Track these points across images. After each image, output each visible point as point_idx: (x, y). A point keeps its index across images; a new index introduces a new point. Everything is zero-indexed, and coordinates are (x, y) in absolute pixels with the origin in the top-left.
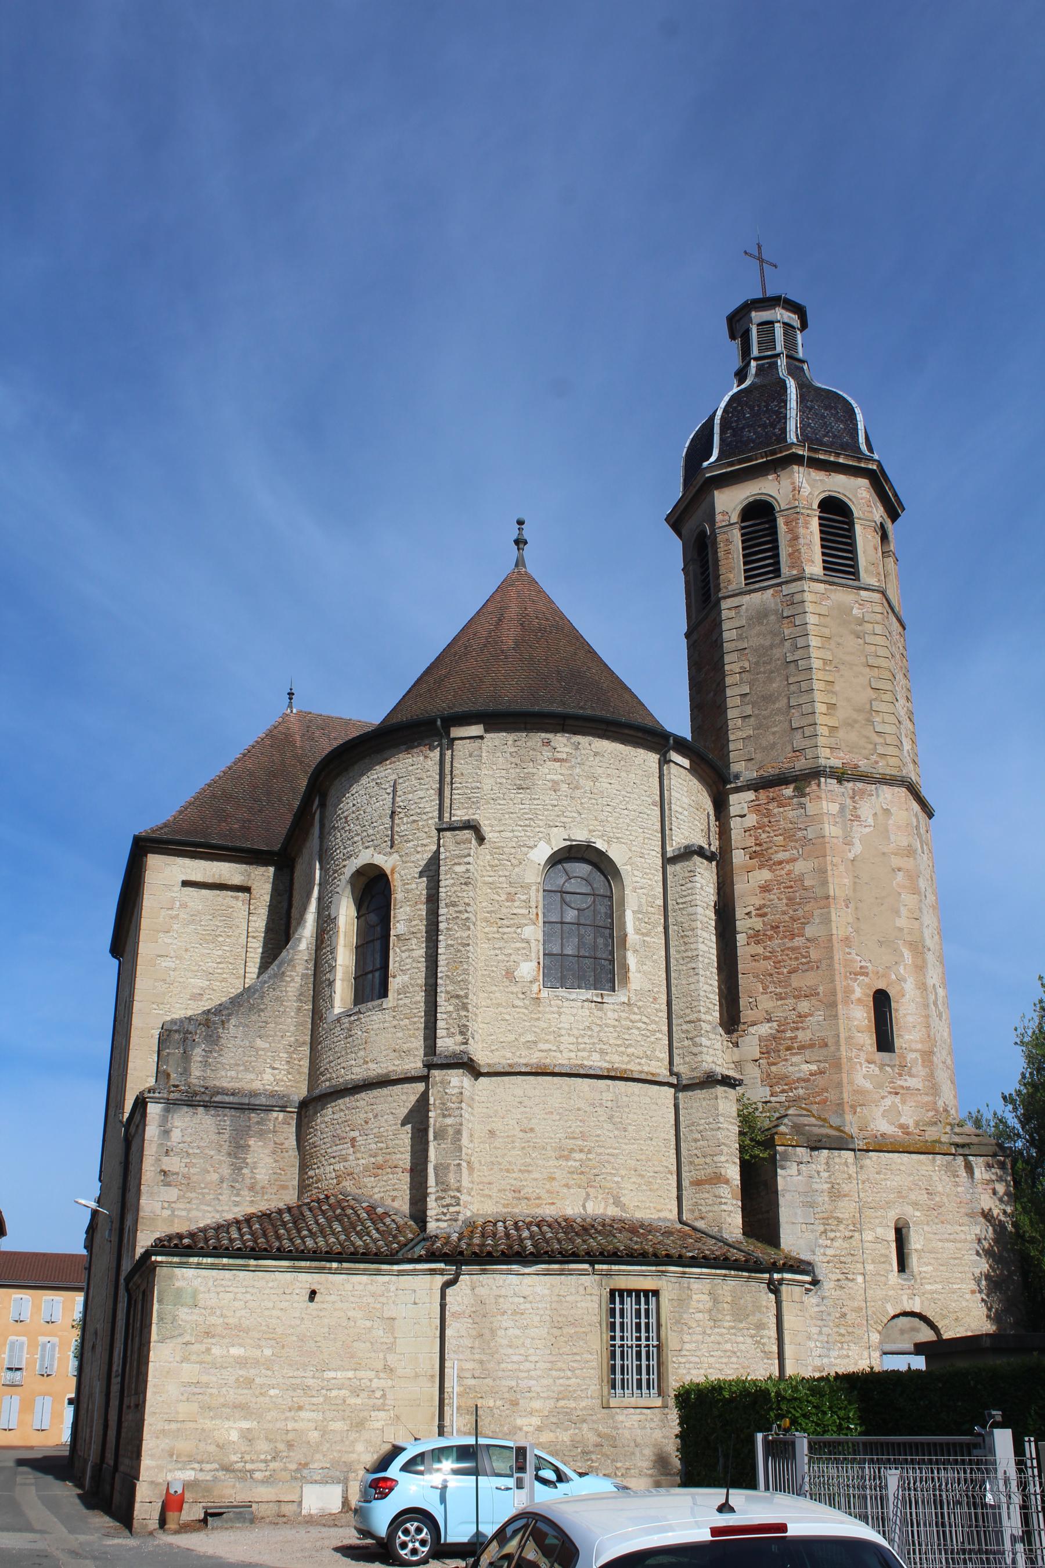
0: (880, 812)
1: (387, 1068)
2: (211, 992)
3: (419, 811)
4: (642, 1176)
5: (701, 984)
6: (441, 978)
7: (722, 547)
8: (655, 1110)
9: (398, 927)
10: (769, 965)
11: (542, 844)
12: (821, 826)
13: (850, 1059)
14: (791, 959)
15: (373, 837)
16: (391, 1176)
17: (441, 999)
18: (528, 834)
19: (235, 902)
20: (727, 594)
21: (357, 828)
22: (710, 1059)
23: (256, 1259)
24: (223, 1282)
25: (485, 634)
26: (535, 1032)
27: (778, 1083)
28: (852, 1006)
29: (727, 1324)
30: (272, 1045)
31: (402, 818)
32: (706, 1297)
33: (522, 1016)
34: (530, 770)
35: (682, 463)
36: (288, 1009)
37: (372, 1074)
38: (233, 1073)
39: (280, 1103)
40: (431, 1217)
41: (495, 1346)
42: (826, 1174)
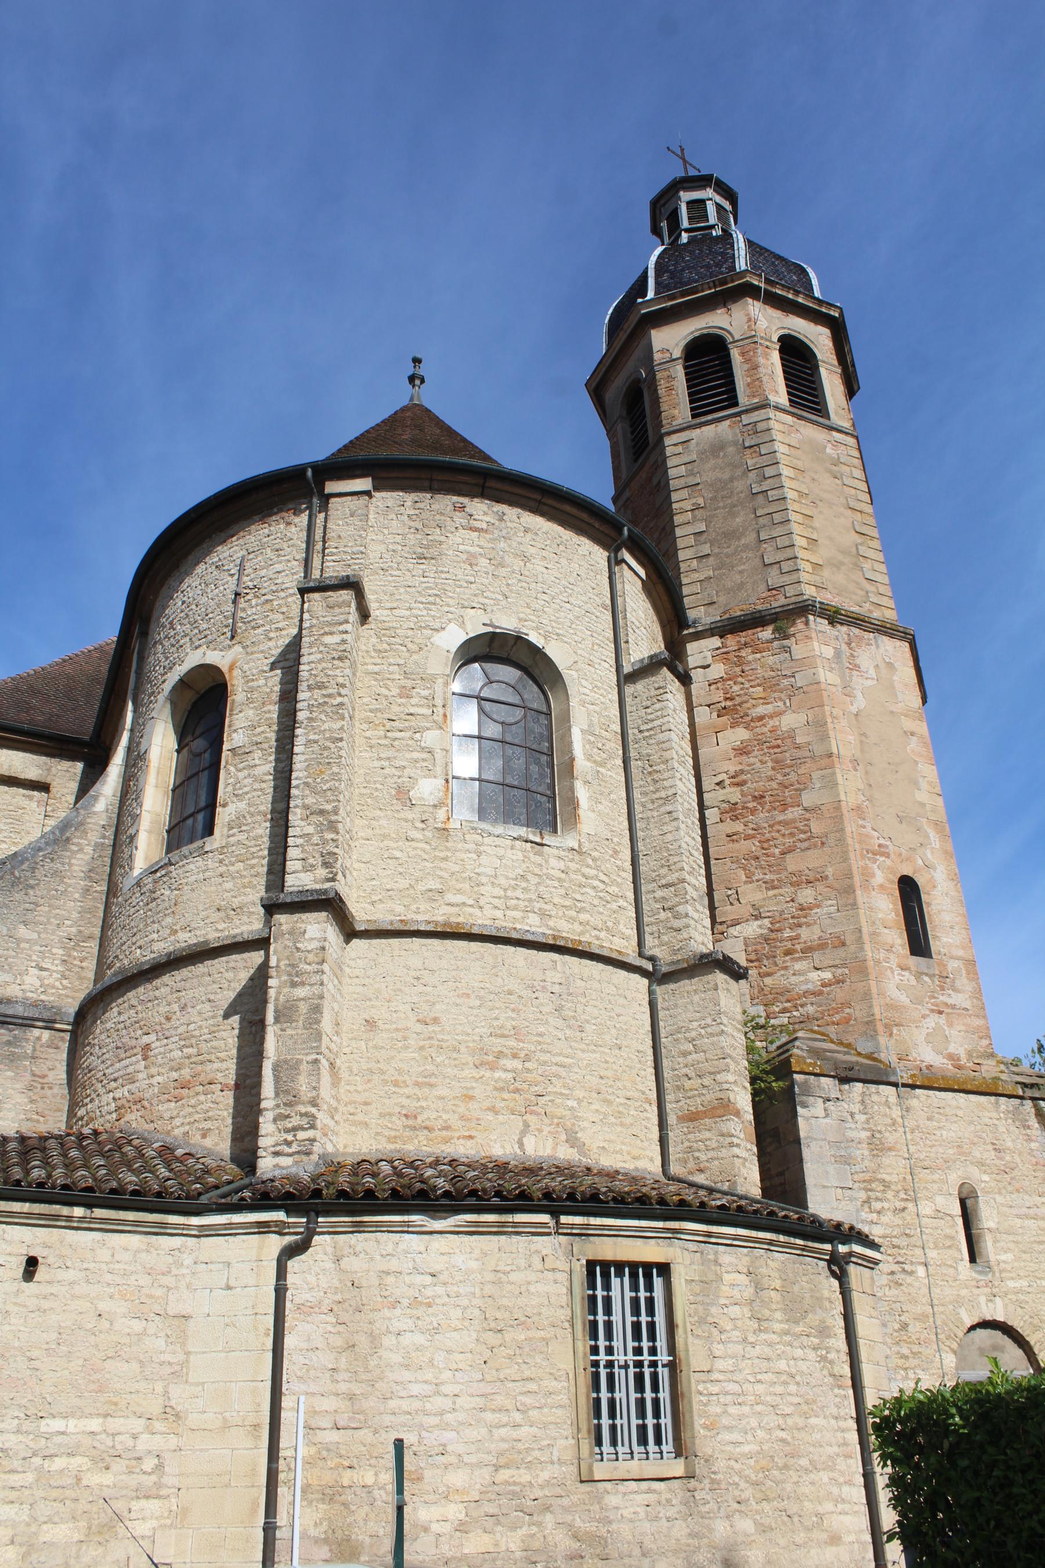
0: (882, 665)
1: (204, 936)
3: (274, 588)
4: (609, 1102)
5: (682, 833)
6: (297, 787)
8: (623, 1006)
9: (235, 737)
10: (752, 846)
11: (452, 627)
12: (813, 670)
13: (878, 962)
14: (784, 835)
16: (202, 1098)
17: (295, 817)
18: (433, 613)
19: (28, 802)
21: (184, 628)
22: (700, 939)
28: (874, 893)
29: (777, 1327)
30: (43, 936)
31: (249, 600)
32: (743, 1279)
33: (420, 852)
34: (437, 537)
36: (70, 889)
39: (46, 1015)
40: (265, 1149)
41: (378, 1366)
42: (862, 1118)
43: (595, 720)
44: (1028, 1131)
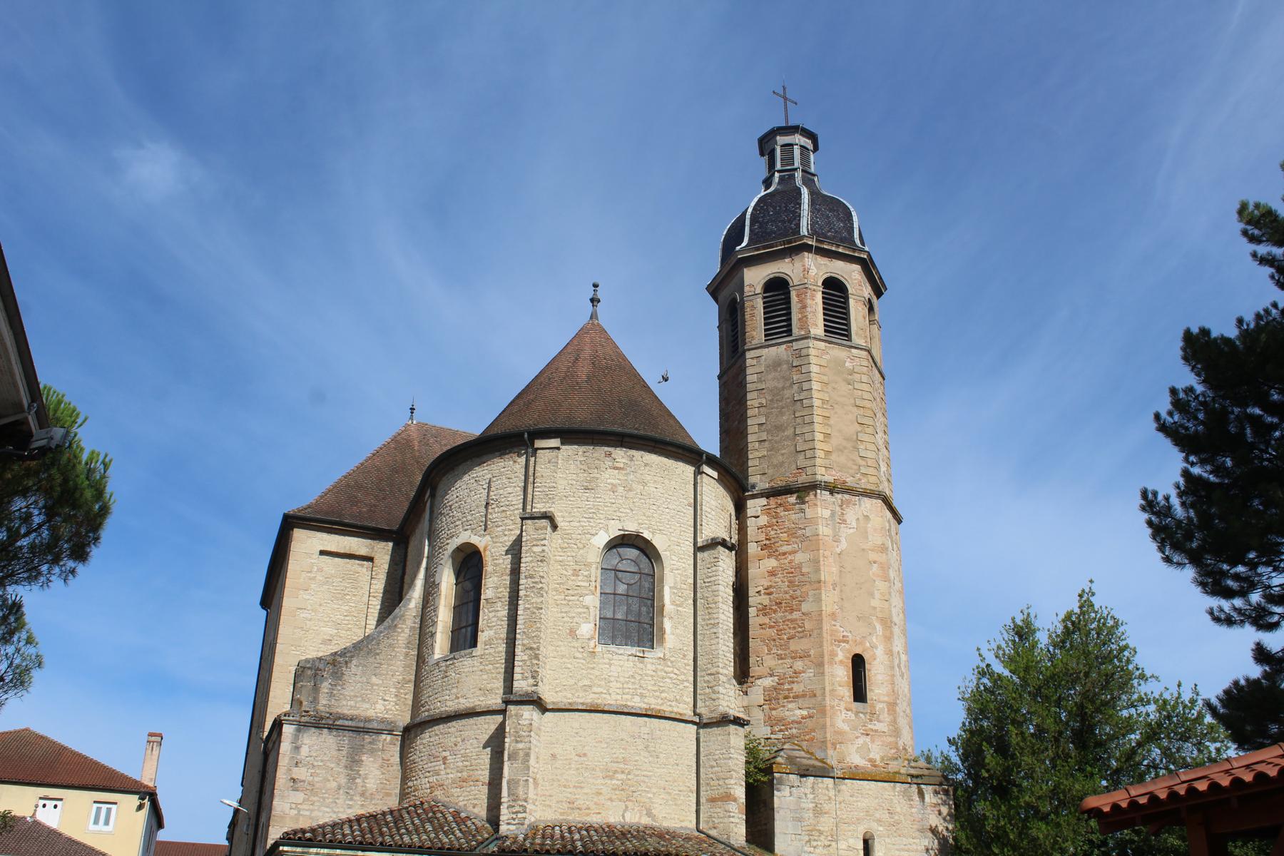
0: (861, 518)
1: (473, 702)
2: (339, 638)
3: (507, 503)
5: (720, 645)
6: (519, 634)
7: (748, 310)
8: (682, 742)
9: (487, 593)
10: (773, 632)
11: (602, 533)
13: (833, 707)
14: (790, 628)
15: (471, 522)
16: (473, 788)
17: (518, 650)
18: (591, 524)
20: (751, 347)
22: (725, 704)
23: (363, 851)
25: (565, 369)
26: (591, 679)
27: (776, 724)
28: (835, 666)
33: (581, 665)
34: (595, 475)
35: (720, 246)
37: (462, 707)
38: (352, 703)
39: (389, 728)
40: (503, 821)
42: (811, 796)
43: (678, 579)
44: (912, 802)
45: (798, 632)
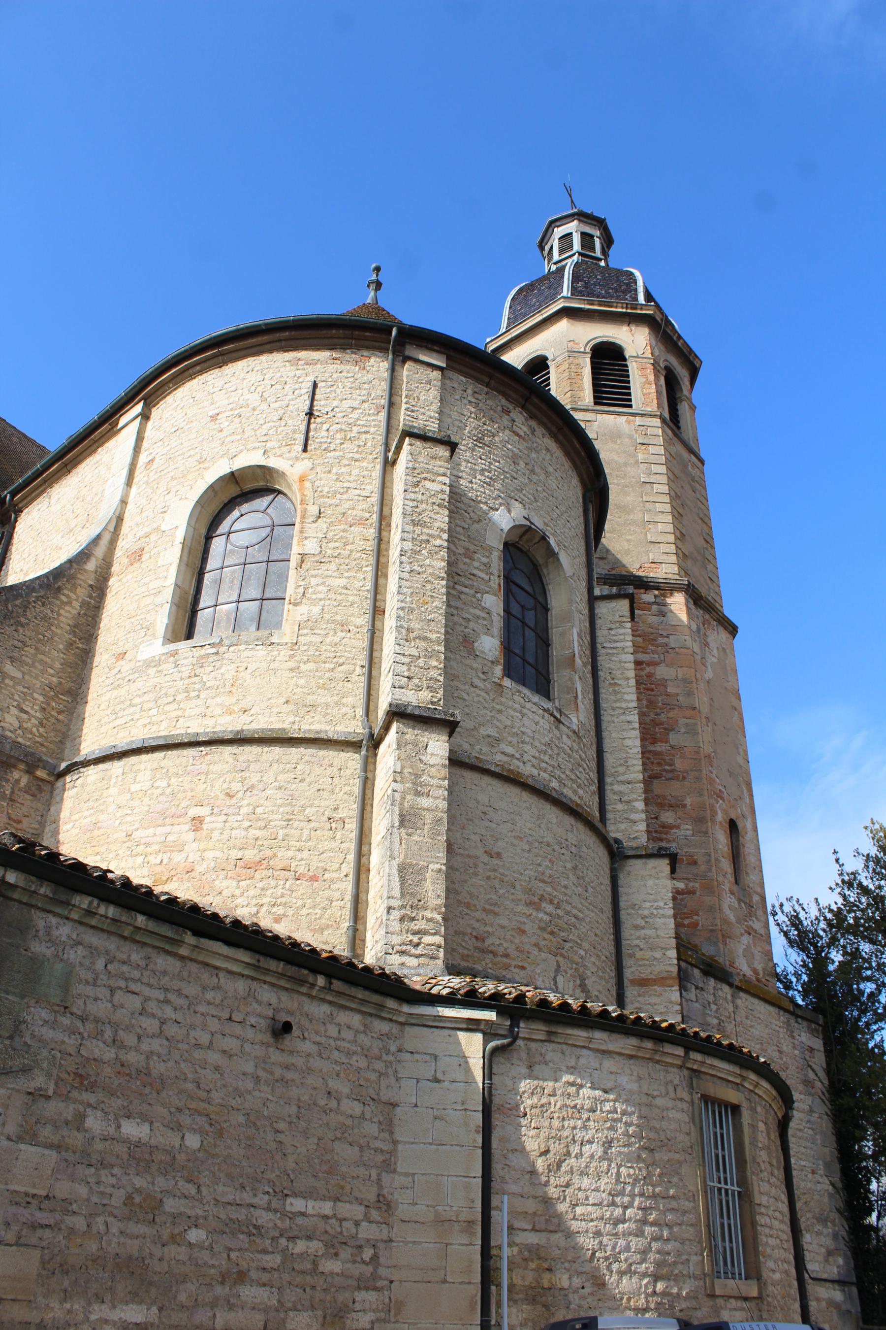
14: (652, 763)
24: (125, 968)
33: (483, 701)
45: (665, 770)
